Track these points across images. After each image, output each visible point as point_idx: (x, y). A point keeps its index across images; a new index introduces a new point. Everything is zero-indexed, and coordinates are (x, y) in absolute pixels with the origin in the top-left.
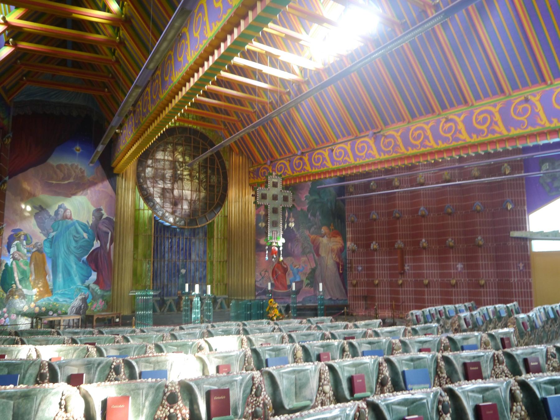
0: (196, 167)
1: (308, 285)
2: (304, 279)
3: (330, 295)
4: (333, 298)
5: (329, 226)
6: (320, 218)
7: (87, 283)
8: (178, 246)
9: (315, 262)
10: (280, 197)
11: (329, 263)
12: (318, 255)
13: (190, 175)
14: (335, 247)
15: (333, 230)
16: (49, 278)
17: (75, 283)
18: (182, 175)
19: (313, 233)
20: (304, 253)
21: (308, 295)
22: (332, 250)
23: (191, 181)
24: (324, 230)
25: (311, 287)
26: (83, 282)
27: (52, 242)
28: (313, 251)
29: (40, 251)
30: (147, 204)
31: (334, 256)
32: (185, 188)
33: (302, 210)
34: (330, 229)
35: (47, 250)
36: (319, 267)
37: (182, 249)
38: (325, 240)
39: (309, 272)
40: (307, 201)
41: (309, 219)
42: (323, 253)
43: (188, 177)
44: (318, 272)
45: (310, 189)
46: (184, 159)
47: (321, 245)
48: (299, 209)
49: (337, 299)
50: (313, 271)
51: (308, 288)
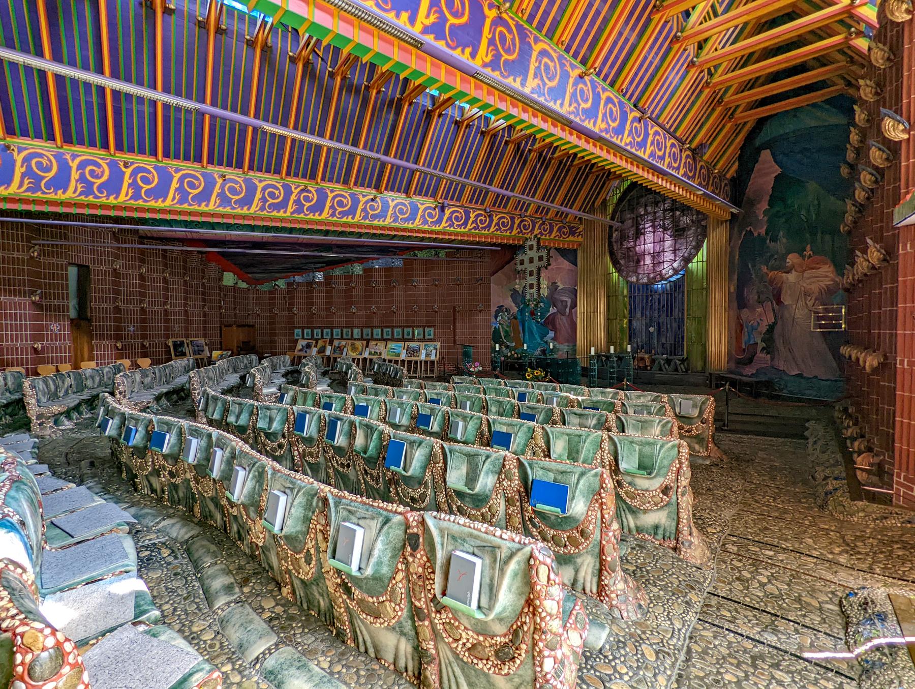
0: (660, 214)
1: (763, 349)
2: (759, 341)
3: (799, 369)
4: (805, 375)
5: (801, 252)
6: (784, 240)
7: (545, 339)
8: (659, 303)
9: (775, 317)
10: (536, 259)
11: (798, 315)
12: (779, 302)
13: (653, 226)
14: (814, 287)
15: (810, 256)
16: (521, 335)
17: (535, 339)
18: (644, 228)
19: (773, 269)
20: (760, 302)
21: (763, 366)
22: (807, 294)
23: (654, 232)
24: (792, 259)
25: (768, 353)
26: (542, 339)
27: (522, 311)
28: (771, 298)
29: (515, 318)
30: (616, 268)
31: (810, 303)
32: (648, 241)
33: (759, 234)
34: (803, 257)
35: (519, 317)
36: (779, 323)
37: (663, 307)
38: (792, 277)
39: (765, 330)
40: (766, 218)
41: (768, 247)
42: (787, 300)
43: (650, 229)
44: (778, 329)
45: (771, 196)
46: (646, 210)
47: (784, 285)
48: (756, 234)
49: (816, 377)
50: (771, 328)
51: (763, 355)
